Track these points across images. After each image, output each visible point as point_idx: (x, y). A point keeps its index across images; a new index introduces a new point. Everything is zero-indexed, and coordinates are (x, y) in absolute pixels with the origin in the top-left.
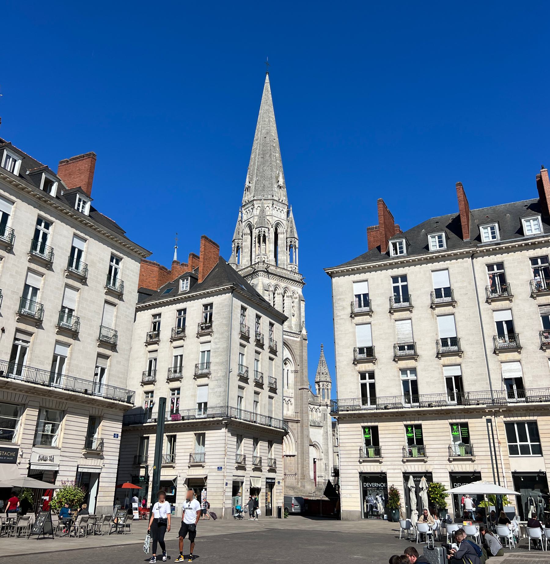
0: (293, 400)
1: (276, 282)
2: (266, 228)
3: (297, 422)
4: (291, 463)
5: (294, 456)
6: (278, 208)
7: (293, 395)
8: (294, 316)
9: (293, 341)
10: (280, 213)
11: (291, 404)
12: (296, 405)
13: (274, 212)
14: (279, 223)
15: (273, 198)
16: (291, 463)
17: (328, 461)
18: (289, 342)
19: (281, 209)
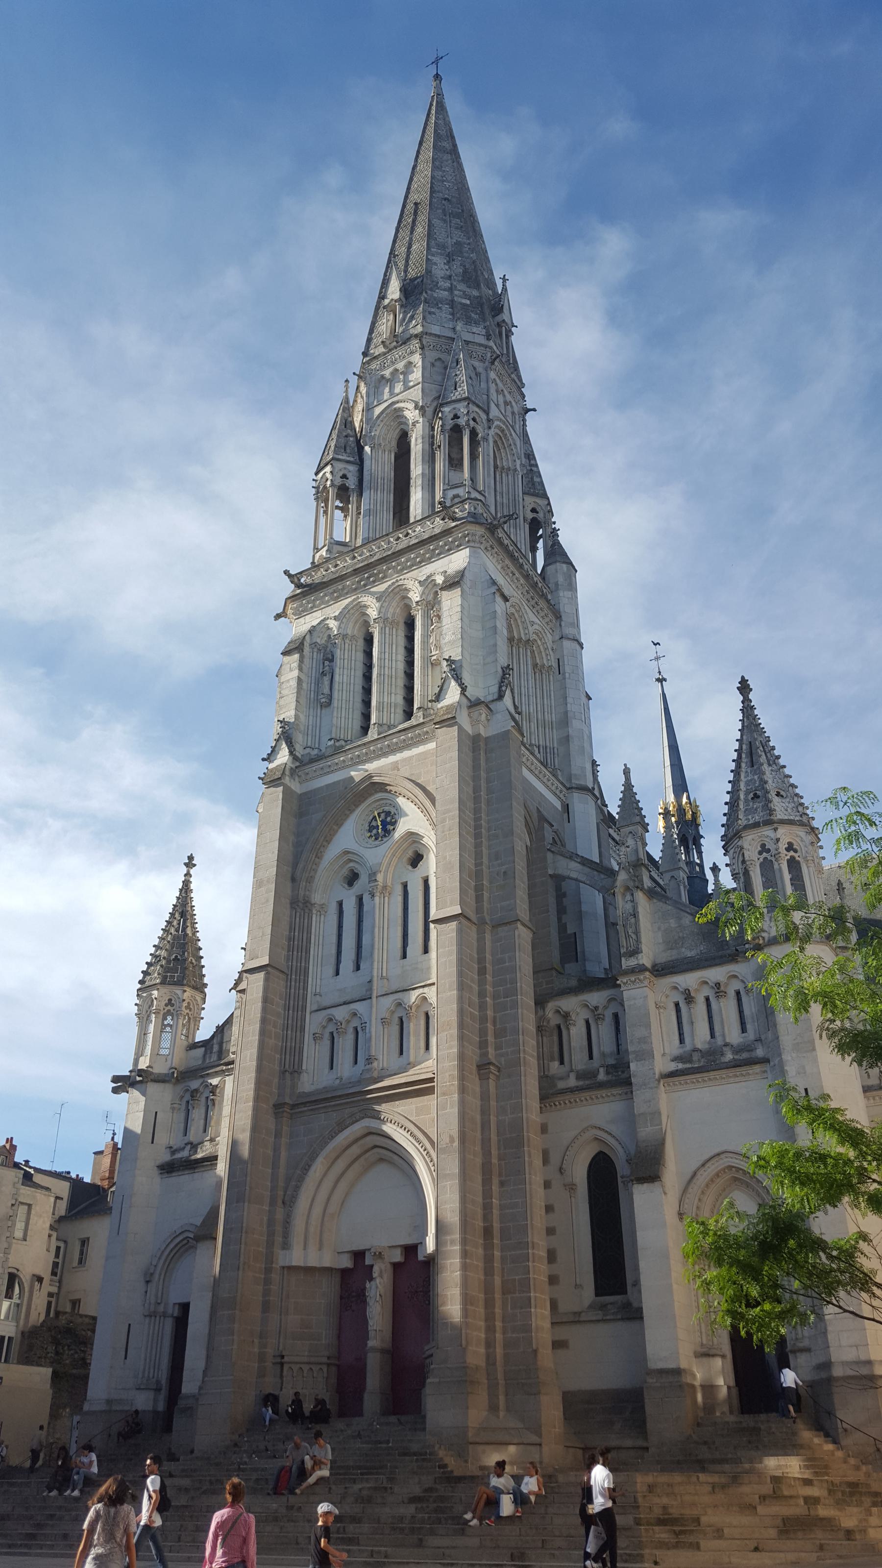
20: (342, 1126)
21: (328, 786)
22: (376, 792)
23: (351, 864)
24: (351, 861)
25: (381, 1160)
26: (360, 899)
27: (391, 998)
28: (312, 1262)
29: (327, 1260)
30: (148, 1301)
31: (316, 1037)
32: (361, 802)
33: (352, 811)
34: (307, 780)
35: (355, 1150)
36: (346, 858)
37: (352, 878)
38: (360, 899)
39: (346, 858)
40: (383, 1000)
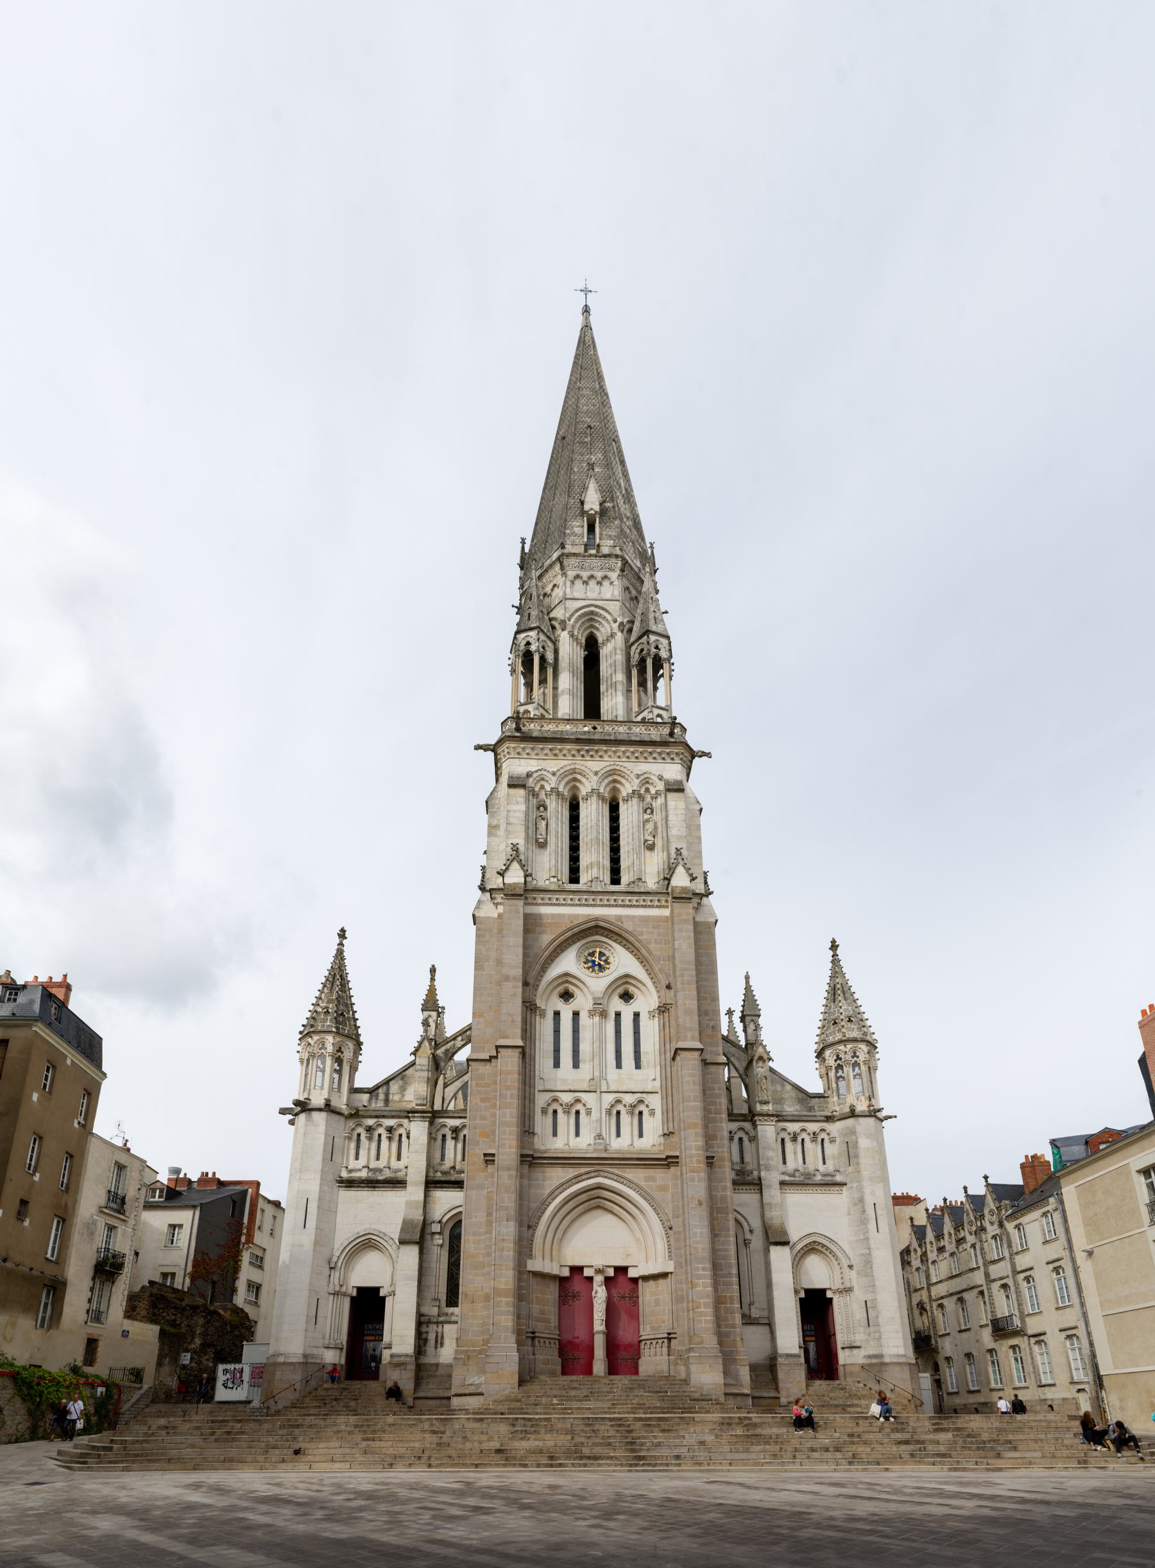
0: (655, 1102)
1: (565, 762)
2: (531, 629)
3: (669, 1162)
4: (657, 1302)
5: (664, 1275)
6: (585, 575)
7: (658, 1083)
8: (651, 848)
9: (645, 919)
10: (597, 588)
11: (652, 1113)
12: (665, 1112)
13: (579, 590)
14: (592, 613)
15: (566, 551)
16: (657, 1302)
17: (874, 1292)
18: (628, 925)
19: (599, 575)
20: (577, 1179)
21: (553, 916)
22: (597, 934)
23: (567, 985)
24: (567, 982)
25: (598, 1207)
26: (576, 1014)
27: (614, 1095)
28: (547, 1270)
29: (555, 1270)
30: (332, 1282)
31: (544, 1111)
32: (583, 938)
33: (574, 943)
34: (533, 904)
35: (584, 1197)
36: (564, 979)
37: (567, 996)
38: (576, 1014)
39: (564, 979)
40: (603, 1094)
